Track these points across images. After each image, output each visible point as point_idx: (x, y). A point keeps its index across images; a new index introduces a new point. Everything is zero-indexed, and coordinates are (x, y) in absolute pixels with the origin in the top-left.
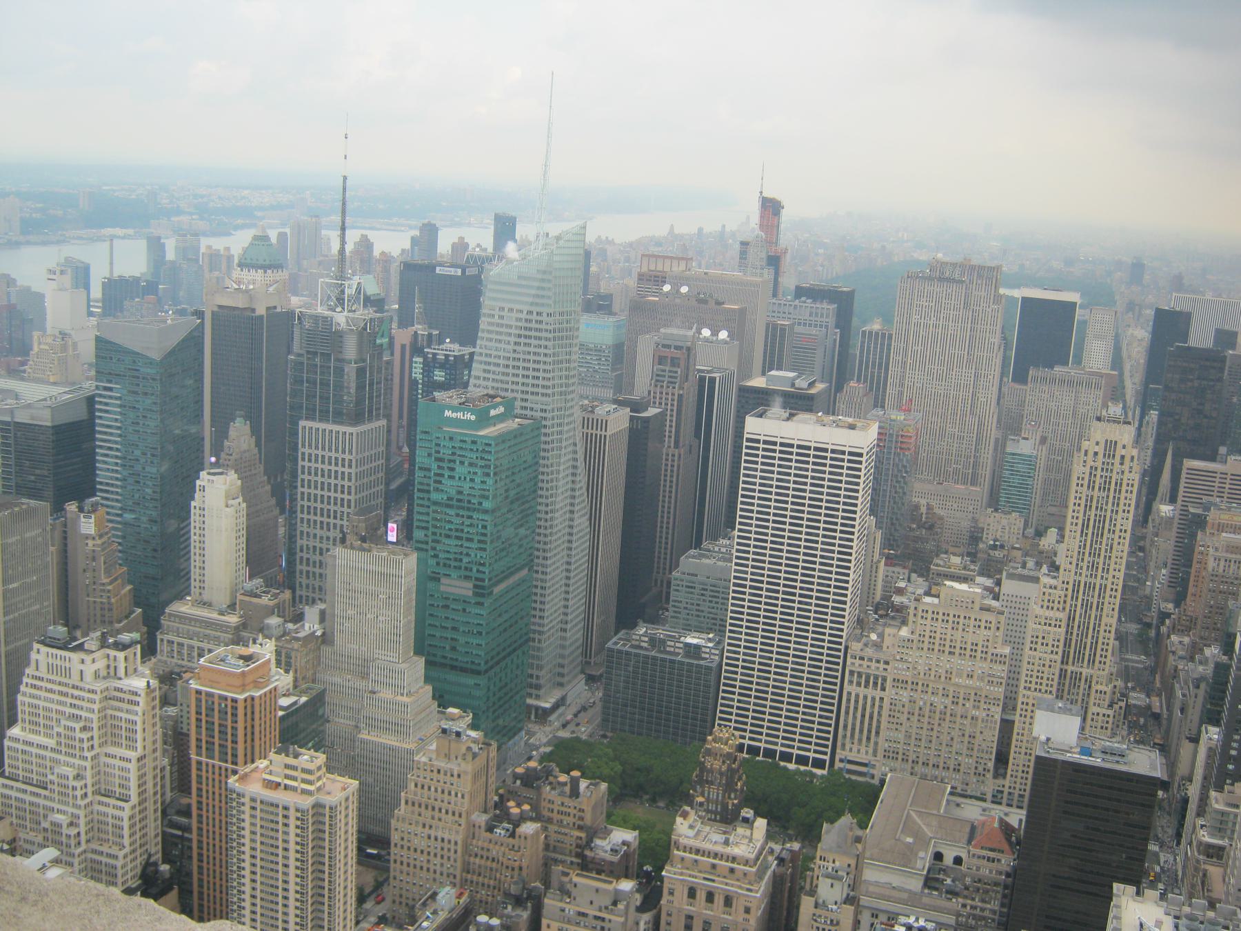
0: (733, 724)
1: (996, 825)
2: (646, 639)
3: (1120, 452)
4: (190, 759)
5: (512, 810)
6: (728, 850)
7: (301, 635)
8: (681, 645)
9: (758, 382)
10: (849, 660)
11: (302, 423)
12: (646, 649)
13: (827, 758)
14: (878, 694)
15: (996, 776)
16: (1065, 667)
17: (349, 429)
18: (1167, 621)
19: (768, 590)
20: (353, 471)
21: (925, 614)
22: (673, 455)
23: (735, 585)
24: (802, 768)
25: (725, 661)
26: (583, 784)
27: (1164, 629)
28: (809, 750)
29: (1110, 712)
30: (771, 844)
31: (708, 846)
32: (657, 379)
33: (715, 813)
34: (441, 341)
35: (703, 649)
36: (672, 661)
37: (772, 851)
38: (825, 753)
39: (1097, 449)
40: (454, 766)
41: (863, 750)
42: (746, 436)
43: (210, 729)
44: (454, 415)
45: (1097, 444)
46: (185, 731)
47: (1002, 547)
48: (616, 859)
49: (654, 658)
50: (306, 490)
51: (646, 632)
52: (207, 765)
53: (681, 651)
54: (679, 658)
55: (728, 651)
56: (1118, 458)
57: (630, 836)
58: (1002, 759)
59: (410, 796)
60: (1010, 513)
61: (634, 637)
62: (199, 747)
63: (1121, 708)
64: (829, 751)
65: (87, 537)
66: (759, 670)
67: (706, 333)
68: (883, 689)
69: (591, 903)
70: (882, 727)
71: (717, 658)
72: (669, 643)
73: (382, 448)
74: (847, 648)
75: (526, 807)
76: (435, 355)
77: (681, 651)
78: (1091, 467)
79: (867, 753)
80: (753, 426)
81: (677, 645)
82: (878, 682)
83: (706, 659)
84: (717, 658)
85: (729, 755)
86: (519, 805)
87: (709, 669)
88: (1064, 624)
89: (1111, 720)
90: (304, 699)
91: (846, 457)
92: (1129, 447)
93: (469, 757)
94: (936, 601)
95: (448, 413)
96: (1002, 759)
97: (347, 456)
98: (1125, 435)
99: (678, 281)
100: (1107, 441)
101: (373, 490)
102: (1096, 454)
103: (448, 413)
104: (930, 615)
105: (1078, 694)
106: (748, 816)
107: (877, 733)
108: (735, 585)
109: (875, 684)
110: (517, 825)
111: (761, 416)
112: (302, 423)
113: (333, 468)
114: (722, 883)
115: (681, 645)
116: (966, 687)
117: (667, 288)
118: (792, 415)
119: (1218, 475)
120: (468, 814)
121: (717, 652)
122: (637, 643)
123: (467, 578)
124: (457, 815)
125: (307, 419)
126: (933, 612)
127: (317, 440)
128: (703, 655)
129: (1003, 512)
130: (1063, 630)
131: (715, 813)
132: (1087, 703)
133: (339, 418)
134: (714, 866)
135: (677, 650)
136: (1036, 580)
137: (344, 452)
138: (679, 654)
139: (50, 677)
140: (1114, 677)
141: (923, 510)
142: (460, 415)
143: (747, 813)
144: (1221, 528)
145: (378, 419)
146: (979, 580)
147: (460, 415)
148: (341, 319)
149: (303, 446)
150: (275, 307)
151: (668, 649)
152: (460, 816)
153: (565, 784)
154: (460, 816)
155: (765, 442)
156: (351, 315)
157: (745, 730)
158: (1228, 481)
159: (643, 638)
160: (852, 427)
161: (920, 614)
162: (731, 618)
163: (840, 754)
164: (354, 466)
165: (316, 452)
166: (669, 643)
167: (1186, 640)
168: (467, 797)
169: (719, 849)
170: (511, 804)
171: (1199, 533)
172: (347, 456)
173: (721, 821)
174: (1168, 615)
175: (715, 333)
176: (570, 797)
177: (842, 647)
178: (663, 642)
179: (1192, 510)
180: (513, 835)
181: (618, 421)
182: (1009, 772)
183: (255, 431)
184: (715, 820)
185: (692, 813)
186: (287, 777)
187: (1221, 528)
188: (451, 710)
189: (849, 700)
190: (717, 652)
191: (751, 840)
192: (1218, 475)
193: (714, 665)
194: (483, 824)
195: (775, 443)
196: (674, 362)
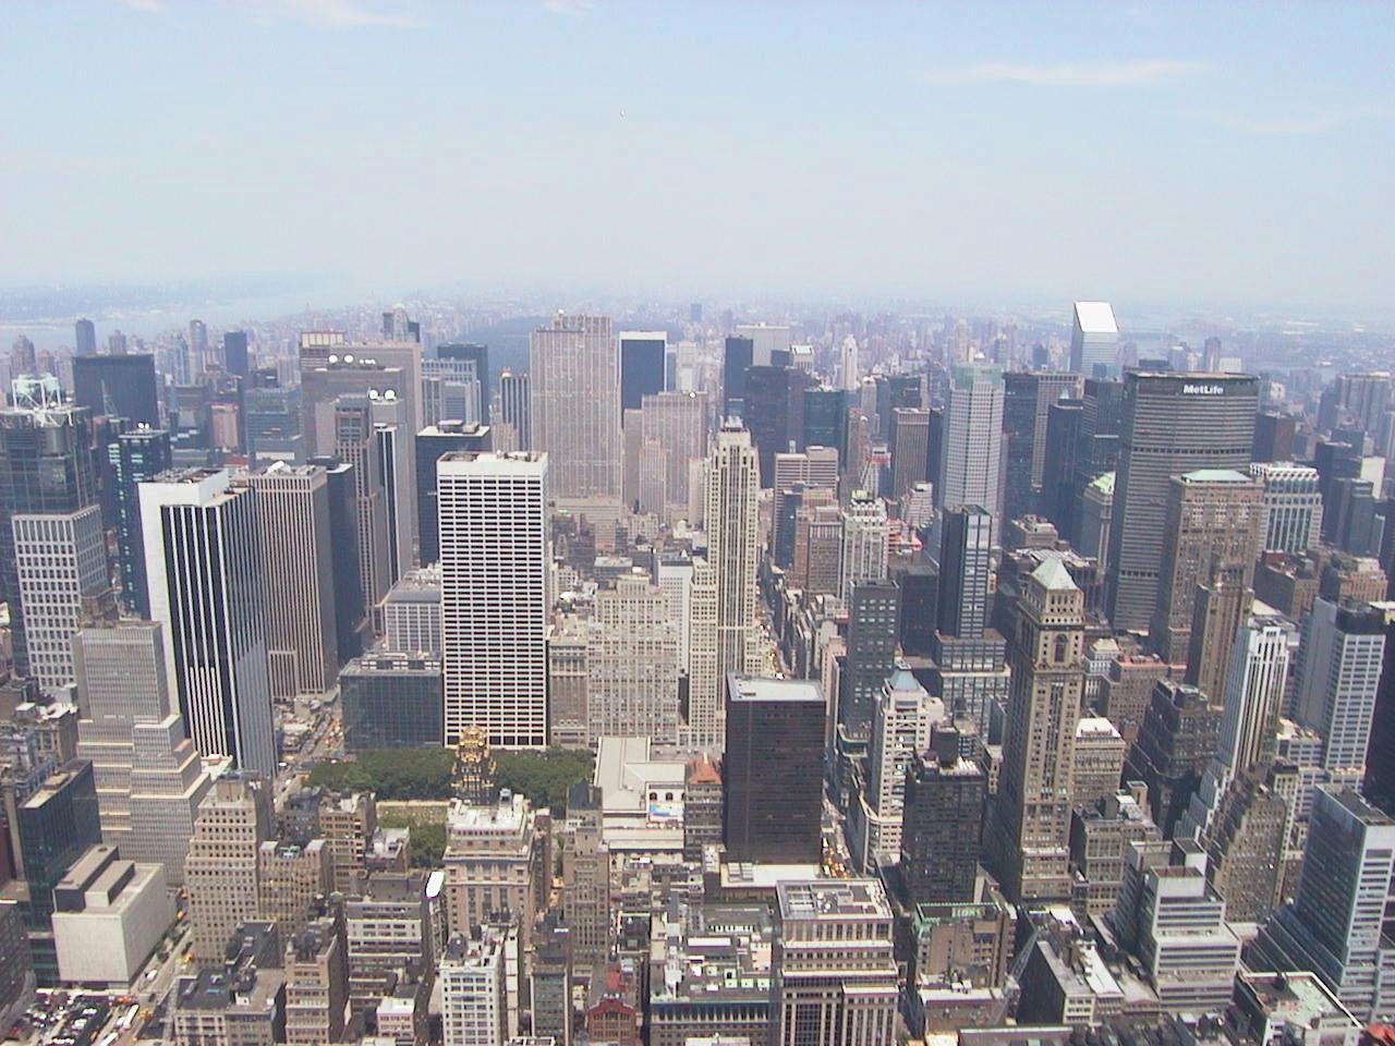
1: (706, 762)
3: (743, 454)
6: (495, 827)
7: (57, 715)
9: (431, 431)
10: (551, 651)
11: (15, 518)
13: (544, 735)
17: (65, 518)
18: (781, 581)
24: (526, 747)
27: (779, 587)
31: (478, 827)
32: (342, 436)
33: (476, 799)
34: (133, 426)
40: (239, 804)
42: (439, 478)
47: (646, 542)
48: (394, 855)
57: (404, 833)
64: (544, 728)
67: (374, 394)
74: (547, 642)
76: (129, 440)
80: (446, 469)
85: (482, 749)
88: (717, 595)
90: (74, 774)
91: (527, 485)
92: (749, 447)
93: (251, 795)
98: (744, 439)
99: (341, 354)
110: (303, 845)
111: (449, 460)
112: (15, 518)
113: (61, 556)
118: (476, 456)
120: (258, 845)
125: (19, 513)
127: (47, 532)
130: (717, 599)
131: (476, 799)
133: (52, 507)
134: (487, 842)
136: (690, 564)
141: (577, 520)
143: (505, 792)
144: (813, 504)
145: (91, 503)
146: (636, 570)
148: (40, 415)
149: (19, 539)
156: (50, 411)
160: (528, 459)
163: (554, 727)
167: (799, 592)
174: (780, 576)
175: (381, 393)
177: (543, 642)
179: (786, 492)
180: (302, 856)
185: (459, 802)
193: (438, 674)
196: (357, 421)
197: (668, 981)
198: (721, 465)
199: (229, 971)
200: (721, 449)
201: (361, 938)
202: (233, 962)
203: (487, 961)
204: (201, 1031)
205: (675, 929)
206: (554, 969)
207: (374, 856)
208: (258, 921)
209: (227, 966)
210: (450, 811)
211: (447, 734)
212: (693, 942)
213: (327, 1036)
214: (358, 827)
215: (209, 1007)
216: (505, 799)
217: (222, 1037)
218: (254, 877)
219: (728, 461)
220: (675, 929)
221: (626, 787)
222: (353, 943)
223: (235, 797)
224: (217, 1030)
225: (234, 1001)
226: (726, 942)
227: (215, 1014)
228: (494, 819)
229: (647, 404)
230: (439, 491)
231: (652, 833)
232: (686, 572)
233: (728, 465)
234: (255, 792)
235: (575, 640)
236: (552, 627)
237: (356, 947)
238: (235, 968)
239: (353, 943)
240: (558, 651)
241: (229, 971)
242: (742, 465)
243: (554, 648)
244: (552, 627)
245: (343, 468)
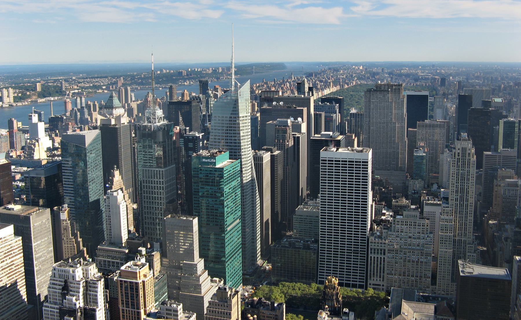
2: (287, 243)
3: (468, 152)
4: (119, 308)
8: (302, 244)
10: (370, 244)
12: (288, 247)
13: (364, 284)
14: (383, 257)
15: (432, 284)
16: (455, 238)
19: (335, 219)
20: (164, 186)
21: (398, 223)
22: (286, 169)
23: (321, 218)
28: (357, 281)
29: (475, 255)
35: (311, 245)
38: (363, 282)
39: (459, 151)
41: (378, 279)
42: (321, 159)
43: (127, 296)
44: (206, 161)
45: (459, 149)
46: (116, 297)
47: (417, 193)
50: (146, 195)
51: (287, 240)
52: (126, 310)
55: (321, 245)
56: (467, 155)
58: (434, 277)
60: (418, 179)
61: (282, 243)
62: (123, 303)
63: (478, 252)
65: (63, 220)
66: (325, 251)
68: (384, 254)
70: (385, 269)
72: (297, 244)
73: (174, 176)
77: (302, 247)
78: (457, 159)
79: (380, 280)
80: (323, 154)
81: (300, 244)
86: (252, 316)
89: (475, 258)
95: (204, 160)
96: (434, 277)
97: (161, 180)
98: (469, 145)
100: (462, 148)
101: (172, 193)
102: (459, 153)
103: (204, 160)
104: (400, 223)
105: (461, 248)
107: (384, 272)
108: (321, 218)
109: (381, 253)
113: (159, 186)
116: (417, 250)
117: (274, 103)
119: (498, 157)
121: (316, 246)
123: (217, 225)
126: (401, 222)
128: (311, 247)
129: (415, 179)
132: (465, 251)
135: (300, 246)
137: (160, 178)
138: (301, 248)
139: (60, 279)
140: (474, 240)
141: (384, 181)
142: (209, 160)
144: (504, 178)
145: (172, 164)
146: (413, 207)
147: (209, 160)
150: (124, 123)
151: (296, 246)
155: (329, 161)
158: (502, 159)
162: (321, 232)
164: (164, 184)
165: (149, 179)
166: (297, 244)
171: (495, 180)
172: (161, 180)
176: (271, 310)
177: (366, 239)
178: (294, 244)
181: (267, 157)
183: (121, 173)
186: (167, 314)
187: (504, 178)
188: (214, 279)
189: (371, 260)
192: (498, 157)
195: (332, 161)
198: (457, 157)
200: (457, 149)
211: (319, 279)
219: (461, 155)
229: (419, 126)
230: (321, 165)
232: (438, 210)
233: (460, 157)
240: (373, 244)
242: (467, 157)
245: (277, 153)
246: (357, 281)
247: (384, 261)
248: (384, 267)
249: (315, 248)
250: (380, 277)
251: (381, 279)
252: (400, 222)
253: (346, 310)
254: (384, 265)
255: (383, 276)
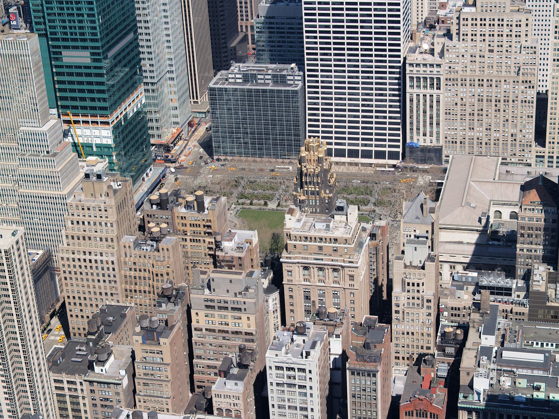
0: (320, 135)
5: (153, 230)
6: (329, 235)
8: (269, 77)
13: (400, 150)
14: (435, 91)
21: (465, 22)
25: (307, 84)
26: (207, 201)
28: (384, 146)
30: (364, 225)
31: (313, 233)
35: (289, 78)
36: (264, 91)
37: (364, 229)
38: (398, 147)
49: (249, 91)
53: (270, 81)
54: (269, 88)
59: (70, 233)
61: (230, 76)
68: (438, 88)
69: (228, 291)
71: (300, 83)
72: (259, 77)
74: (405, 59)
75: (164, 225)
81: (267, 77)
82: (436, 83)
83: (291, 85)
84: (300, 83)
87: (296, 92)
93: (111, 193)
94: (473, 9)
106: (341, 205)
109: (432, 85)
114: (329, 260)
115: (269, 77)
120: (118, 238)
121: (300, 78)
122: (233, 80)
124: (109, 240)
128: (289, 82)
134: (320, 248)
135: (267, 81)
151: (259, 81)
152: (112, 240)
153: (192, 202)
154: (112, 240)
157: (331, 138)
159: (238, 76)
161: (462, 22)
166: (259, 77)
168: (114, 225)
169: (323, 234)
170: (151, 225)
173: (322, 212)
177: (402, 59)
178: (254, 76)
182: (547, 141)
184: (316, 212)
189: (411, 100)
190: (300, 78)
191: (346, 224)
194: (132, 245)
197: (475, 386)
199: (91, 344)
201: (203, 324)
202: (94, 337)
203: (308, 354)
204: (66, 392)
205: (489, 341)
206: (369, 367)
207: (223, 254)
208: (121, 304)
209: (91, 340)
210: (287, 216)
212: (506, 355)
213: (170, 407)
214: (209, 227)
215: (71, 372)
216: (340, 209)
217: (84, 398)
218: (116, 266)
220: (489, 341)
221: (469, 204)
222: (195, 329)
223: (98, 195)
224: (79, 391)
225: (92, 369)
226: (540, 358)
227: (77, 379)
228: (328, 226)
231: (491, 250)
234: (115, 191)
235: (429, 59)
236: (412, 44)
237: (199, 332)
238: (96, 342)
239: (195, 329)
240: (415, 69)
241: (91, 344)
243: (411, 65)
244: (412, 44)
246: (384, 146)
247: (438, 102)
248: (438, 115)
249: (296, 82)
250: (431, 136)
251: (434, 138)
252: (470, 19)
253: (340, 202)
254: (438, 110)
255: (438, 133)
